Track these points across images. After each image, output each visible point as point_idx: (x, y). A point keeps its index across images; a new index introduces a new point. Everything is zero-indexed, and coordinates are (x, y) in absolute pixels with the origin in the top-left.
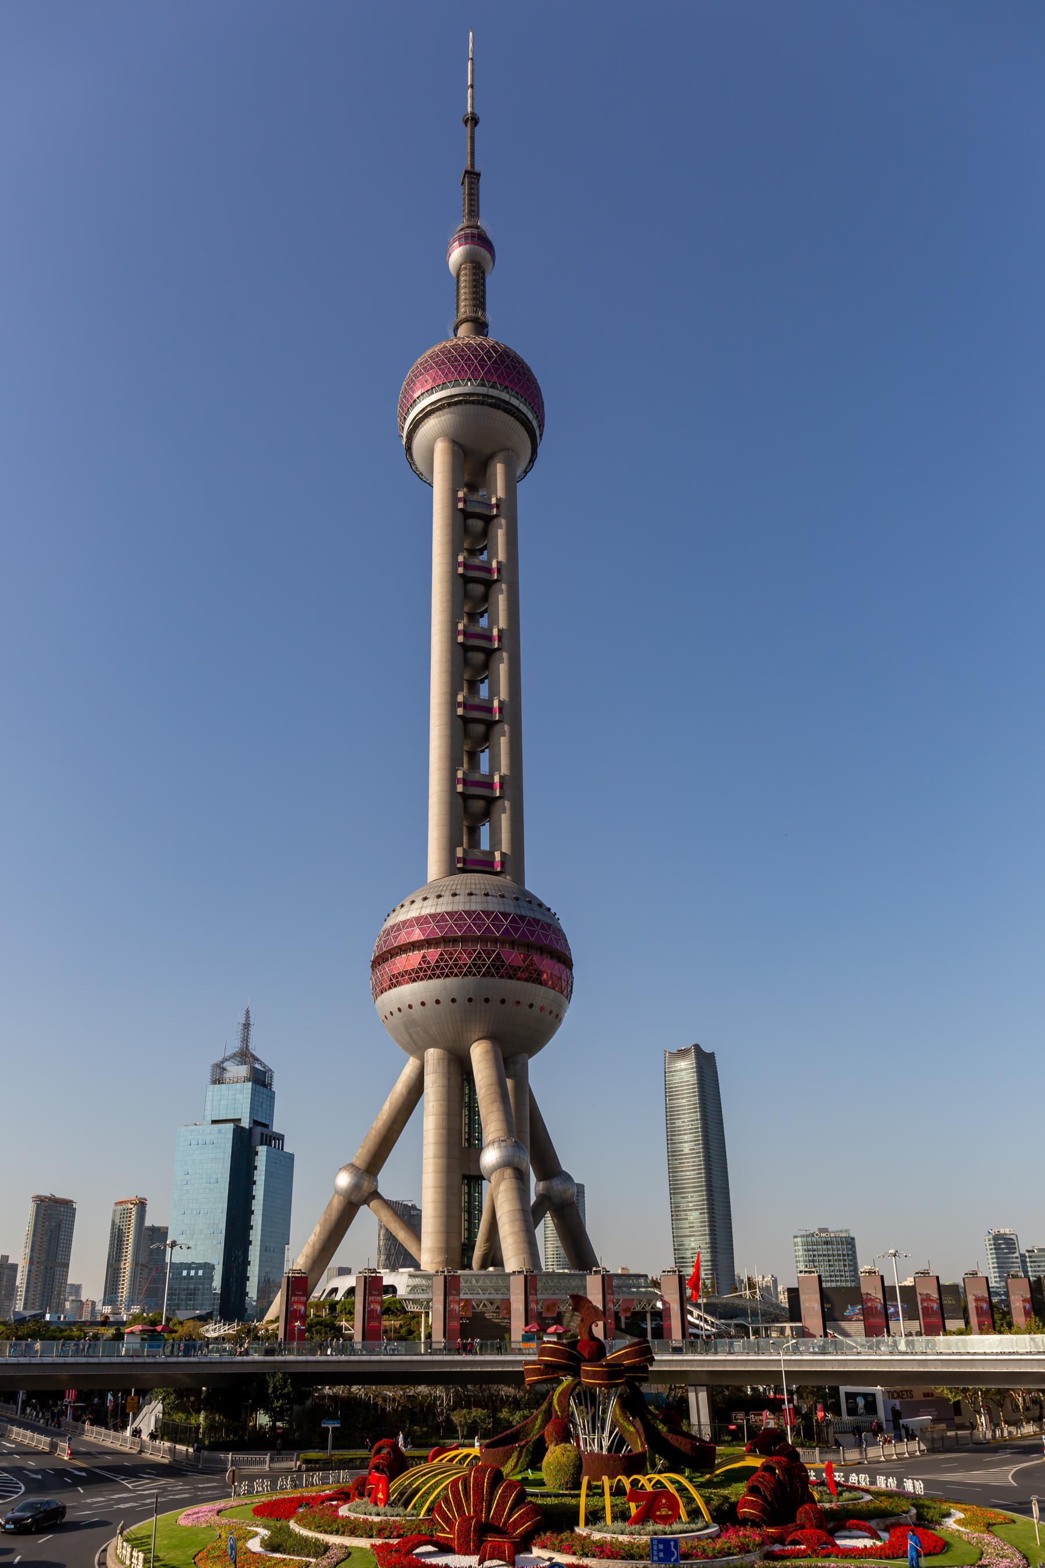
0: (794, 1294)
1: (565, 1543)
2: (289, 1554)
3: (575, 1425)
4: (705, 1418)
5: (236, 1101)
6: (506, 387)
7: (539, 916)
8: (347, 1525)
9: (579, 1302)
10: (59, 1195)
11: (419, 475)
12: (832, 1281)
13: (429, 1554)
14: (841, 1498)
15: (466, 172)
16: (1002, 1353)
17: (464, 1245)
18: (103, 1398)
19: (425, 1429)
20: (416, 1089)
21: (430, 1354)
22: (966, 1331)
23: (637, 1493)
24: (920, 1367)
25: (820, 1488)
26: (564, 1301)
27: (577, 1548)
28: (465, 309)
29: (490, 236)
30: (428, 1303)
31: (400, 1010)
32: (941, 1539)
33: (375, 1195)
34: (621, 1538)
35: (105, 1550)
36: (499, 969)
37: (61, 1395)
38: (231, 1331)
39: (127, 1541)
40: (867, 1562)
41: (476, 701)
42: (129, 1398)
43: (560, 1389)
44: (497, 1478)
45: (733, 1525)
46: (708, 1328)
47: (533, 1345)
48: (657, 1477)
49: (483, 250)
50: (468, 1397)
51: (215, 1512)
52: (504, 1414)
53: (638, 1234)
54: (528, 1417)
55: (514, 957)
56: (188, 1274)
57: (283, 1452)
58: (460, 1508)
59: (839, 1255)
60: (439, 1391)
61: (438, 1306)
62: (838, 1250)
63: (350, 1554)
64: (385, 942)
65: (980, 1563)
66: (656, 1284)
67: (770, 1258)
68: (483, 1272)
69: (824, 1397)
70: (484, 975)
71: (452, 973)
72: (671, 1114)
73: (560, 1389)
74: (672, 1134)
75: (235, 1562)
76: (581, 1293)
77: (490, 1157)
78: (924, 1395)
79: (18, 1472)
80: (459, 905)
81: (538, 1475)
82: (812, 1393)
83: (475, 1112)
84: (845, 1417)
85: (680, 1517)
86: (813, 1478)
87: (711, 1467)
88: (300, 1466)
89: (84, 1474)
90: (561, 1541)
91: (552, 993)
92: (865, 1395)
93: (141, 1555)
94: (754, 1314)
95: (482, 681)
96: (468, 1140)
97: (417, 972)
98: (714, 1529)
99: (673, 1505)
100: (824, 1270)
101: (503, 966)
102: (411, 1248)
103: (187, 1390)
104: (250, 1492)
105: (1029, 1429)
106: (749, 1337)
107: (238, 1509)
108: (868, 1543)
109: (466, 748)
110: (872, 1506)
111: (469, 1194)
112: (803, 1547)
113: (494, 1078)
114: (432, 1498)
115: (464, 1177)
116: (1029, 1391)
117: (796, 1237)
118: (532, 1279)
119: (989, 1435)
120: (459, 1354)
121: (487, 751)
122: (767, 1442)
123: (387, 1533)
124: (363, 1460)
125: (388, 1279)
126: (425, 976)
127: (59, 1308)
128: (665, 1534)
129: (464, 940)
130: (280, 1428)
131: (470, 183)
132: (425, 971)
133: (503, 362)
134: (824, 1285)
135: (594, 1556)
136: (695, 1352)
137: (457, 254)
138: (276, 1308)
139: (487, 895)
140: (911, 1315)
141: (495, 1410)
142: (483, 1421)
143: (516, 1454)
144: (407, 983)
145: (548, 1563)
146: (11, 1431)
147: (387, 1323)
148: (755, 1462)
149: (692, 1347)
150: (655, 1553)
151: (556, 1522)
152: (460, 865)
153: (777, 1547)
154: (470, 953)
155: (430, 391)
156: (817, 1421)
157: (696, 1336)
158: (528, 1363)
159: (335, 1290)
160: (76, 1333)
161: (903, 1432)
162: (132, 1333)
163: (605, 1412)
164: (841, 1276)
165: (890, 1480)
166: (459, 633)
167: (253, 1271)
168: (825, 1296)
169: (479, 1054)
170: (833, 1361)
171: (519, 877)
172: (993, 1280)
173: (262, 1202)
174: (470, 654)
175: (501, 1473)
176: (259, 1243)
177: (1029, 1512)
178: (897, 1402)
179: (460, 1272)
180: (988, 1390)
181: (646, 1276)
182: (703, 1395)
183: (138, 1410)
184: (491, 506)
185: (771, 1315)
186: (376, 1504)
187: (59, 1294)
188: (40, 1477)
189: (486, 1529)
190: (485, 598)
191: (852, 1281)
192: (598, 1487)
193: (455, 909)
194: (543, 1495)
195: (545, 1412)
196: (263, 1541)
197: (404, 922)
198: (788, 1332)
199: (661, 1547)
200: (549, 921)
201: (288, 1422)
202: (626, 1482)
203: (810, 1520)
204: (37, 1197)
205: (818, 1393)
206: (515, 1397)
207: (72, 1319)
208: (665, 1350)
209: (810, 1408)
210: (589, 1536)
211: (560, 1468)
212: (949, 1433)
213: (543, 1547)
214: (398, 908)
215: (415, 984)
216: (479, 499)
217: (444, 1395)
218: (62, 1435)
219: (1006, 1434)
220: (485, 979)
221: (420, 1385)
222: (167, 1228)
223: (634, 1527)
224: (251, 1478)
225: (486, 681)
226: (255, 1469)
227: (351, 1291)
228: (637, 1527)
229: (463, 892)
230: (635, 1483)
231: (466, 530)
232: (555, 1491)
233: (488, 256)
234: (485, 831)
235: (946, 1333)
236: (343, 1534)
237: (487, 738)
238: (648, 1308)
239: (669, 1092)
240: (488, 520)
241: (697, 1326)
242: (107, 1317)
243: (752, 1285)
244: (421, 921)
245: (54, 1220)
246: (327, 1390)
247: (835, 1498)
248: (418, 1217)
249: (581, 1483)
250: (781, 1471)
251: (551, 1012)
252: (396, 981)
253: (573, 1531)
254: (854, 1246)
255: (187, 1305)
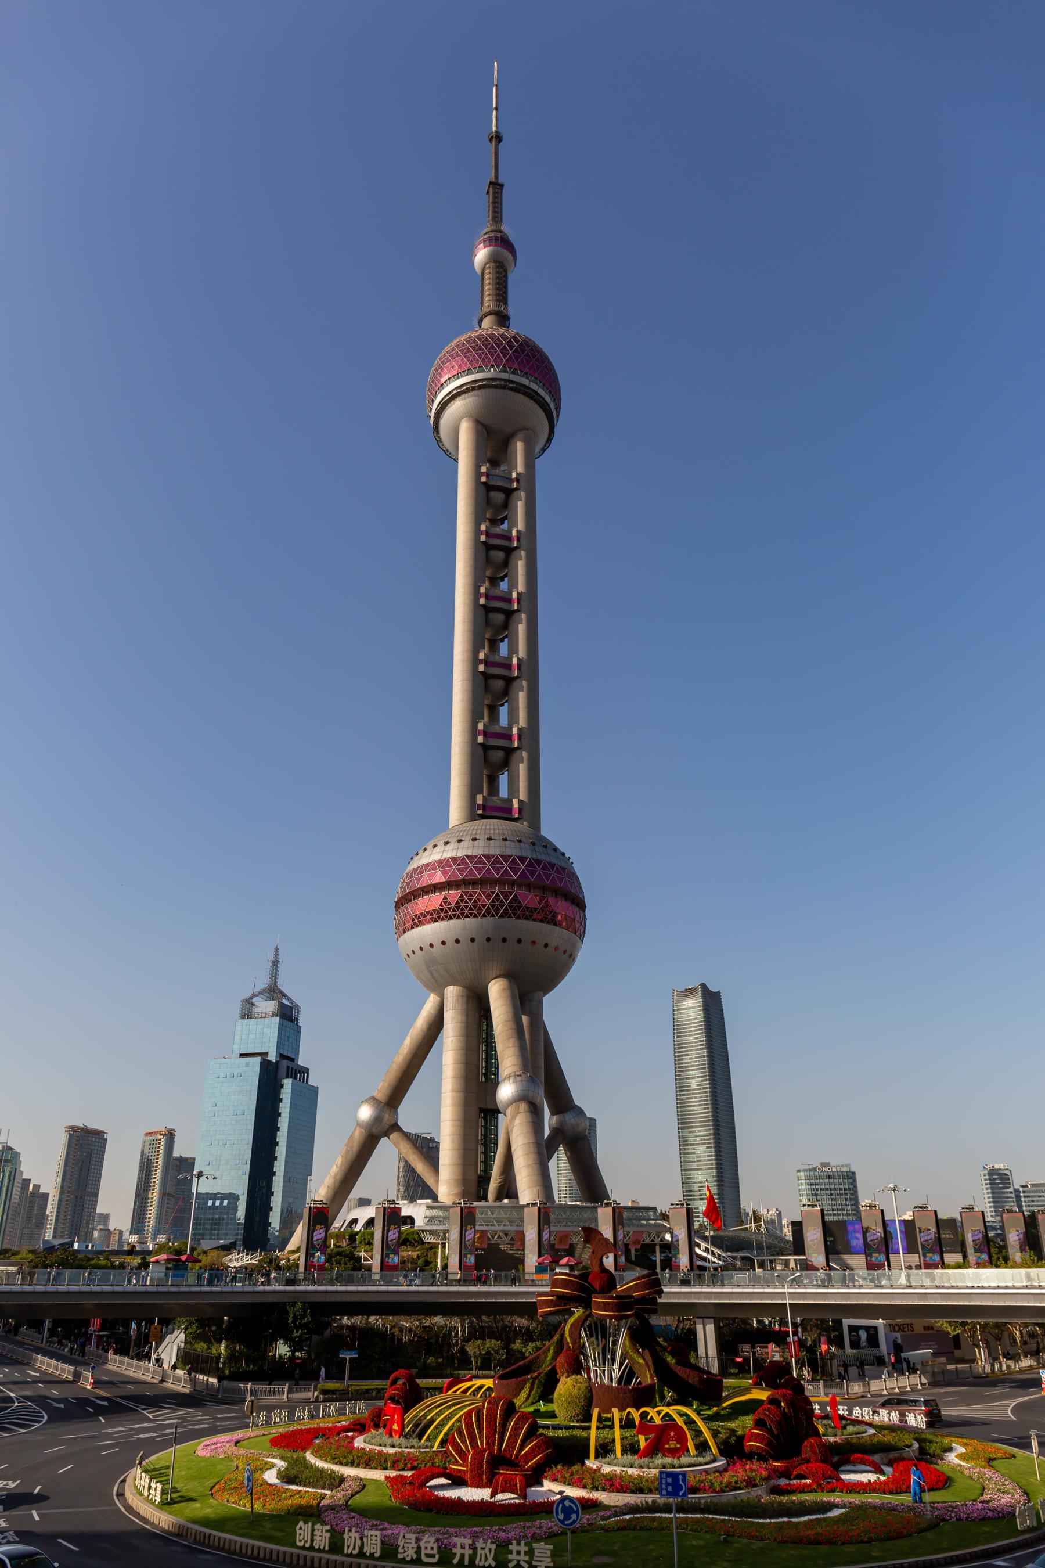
0: (797, 1227)
1: (576, 1477)
2: (305, 1486)
3: (586, 1357)
4: (712, 1351)
5: (264, 1034)
6: (526, 373)
7: (554, 861)
8: (362, 1457)
9: (591, 1234)
10: (91, 1126)
11: (446, 452)
12: (834, 1215)
13: (442, 1487)
14: (845, 1432)
15: (491, 183)
16: (998, 1287)
17: (480, 1177)
18: (128, 1327)
19: (440, 1360)
20: (436, 1025)
21: (446, 1285)
22: (964, 1265)
23: (646, 1426)
24: (919, 1300)
25: (825, 1422)
26: (576, 1233)
27: (587, 1481)
28: (488, 303)
29: (512, 239)
30: (445, 1234)
31: (421, 948)
32: (943, 1473)
33: (395, 1127)
34: (630, 1471)
35: (124, 1481)
36: (517, 910)
37: (86, 1323)
38: (253, 1261)
39: (146, 1471)
40: (871, 1497)
41: (496, 659)
42: (152, 1327)
43: (571, 1320)
44: (510, 1409)
45: (740, 1458)
46: (715, 1260)
47: (546, 1277)
48: (666, 1410)
49: (505, 251)
50: (483, 1327)
51: (233, 1443)
52: (517, 1345)
53: (647, 1167)
54: (540, 1349)
55: (530, 899)
56: (214, 1204)
57: (301, 1382)
58: (473, 1440)
59: (841, 1189)
60: (454, 1322)
61: (454, 1235)
62: (840, 1184)
63: (364, 1486)
64: (408, 883)
65: (982, 1498)
66: (665, 1217)
67: (774, 1194)
68: (498, 1204)
69: (827, 1329)
71: (471, 914)
72: (679, 1050)
73: (571, 1320)
74: (680, 1070)
75: (251, 1494)
76: (593, 1226)
77: (506, 1091)
78: (925, 1328)
79: (42, 1401)
80: (479, 849)
81: (551, 1407)
82: (816, 1326)
83: (492, 1047)
84: (849, 1351)
85: (688, 1451)
86: (817, 1412)
87: (718, 1399)
88: (317, 1397)
89: (106, 1403)
90: (572, 1474)
91: (566, 933)
92: (867, 1328)
93: (159, 1486)
94: (760, 1247)
95: (502, 640)
96: (485, 1075)
97: (438, 913)
98: (721, 1462)
99: (682, 1438)
100: (826, 1203)
102: (430, 1181)
103: (209, 1319)
104: (267, 1423)
105: (1026, 1362)
106: (754, 1270)
107: (257, 1439)
108: (872, 1477)
109: (487, 702)
110: (875, 1440)
111: (486, 1127)
112: (808, 1481)
113: (511, 1015)
114: (446, 1429)
115: (481, 1110)
116: (1026, 1325)
117: (799, 1171)
118: (545, 1212)
119: (988, 1369)
120: (475, 1285)
121: (506, 705)
122: (773, 1375)
123: (401, 1465)
124: (379, 1390)
125: (407, 1210)
126: (446, 916)
127: (87, 1237)
128: (674, 1467)
129: (483, 882)
130: (298, 1358)
131: (494, 193)
132: (446, 911)
133: (523, 351)
134: (827, 1218)
135: (604, 1490)
136: (701, 1285)
137: (481, 255)
138: (298, 1238)
139: (505, 840)
140: (910, 1249)
141: (508, 1341)
142: (497, 1352)
143: (528, 1385)
144: (429, 923)
145: (559, 1497)
146: (36, 1360)
147: (404, 1254)
148: (761, 1395)
149: (700, 1280)
150: (664, 1486)
151: (567, 1454)
152: (480, 812)
153: (783, 1482)
154: (489, 895)
155: (456, 376)
156: (821, 1353)
157: (703, 1269)
158: (540, 1294)
159: (355, 1221)
160: (103, 1262)
161: (905, 1366)
162: (157, 1262)
163: (615, 1343)
164: (843, 1210)
165: (893, 1414)
166: (481, 595)
167: (277, 1202)
168: (827, 1229)
169: (496, 992)
170: (836, 1293)
171: (535, 824)
172: (989, 1214)
173: (286, 1134)
174: (492, 615)
175: (514, 1404)
176: (282, 1174)
177: (1028, 1447)
178: (898, 1335)
179: (475, 1204)
180: (986, 1324)
181: (655, 1209)
182: (710, 1328)
183: (160, 1340)
184: (511, 480)
185: (775, 1248)
186: (391, 1436)
187: (88, 1223)
188: (62, 1406)
189: (499, 1461)
190: (506, 564)
191: (853, 1215)
192: (607, 1419)
193: (475, 853)
194: (555, 1428)
195: (557, 1343)
196: (279, 1473)
197: (427, 865)
198: (792, 1265)
199: (670, 1480)
200: (564, 865)
201: (308, 1352)
202: (636, 1415)
203: (815, 1453)
204: (70, 1127)
205: (822, 1326)
206: (528, 1328)
207: (99, 1248)
208: (672, 1281)
209: (814, 1341)
210: (599, 1469)
211: (571, 1400)
212: (950, 1367)
213: (554, 1480)
214: (421, 851)
215: (437, 924)
216: (501, 474)
217: (459, 1325)
218: (86, 1364)
219: (1004, 1368)
221: (435, 1315)
222: (194, 1159)
223: (643, 1460)
224: (270, 1409)
225: (506, 640)
226: (273, 1399)
227: (371, 1222)
228: (646, 1460)
229: (482, 837)
230: (644, 1415)
231: (488, 502)
232: (566, 1423)
233: (510, 256)
234: (503, 779)
235: (944, 1266)
236: (358, 1466)
237: (506, 693)
238: (657, 1241)
239: (677, 1029)
240: (509, 492)
241: (704, 1259)
242: (134, 1246)
243: (757, 1218)
244: (442, 864)
245: (85, 1150)
246: (345, 1321)
247: (839, 1432)
248: (437, 1149)
249: (591, 1416)
250: (786, 1404)
251: (565, 952)
252: (418, 921)
253: (583, 1464)
254: (855, 1181)
255: (211, 1234)
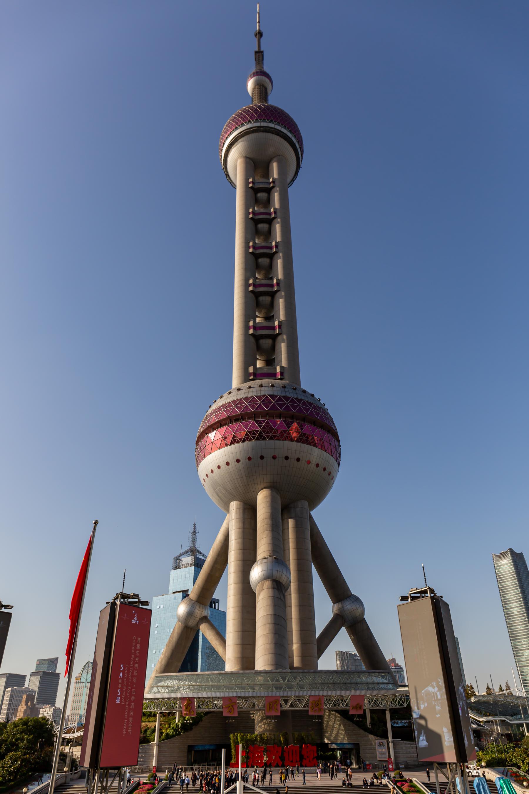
7: (300, 397)
70: (258, 439)
91: (326, 455)
101: (271, 431)
220: (258, 442)
233: (267, 80)
